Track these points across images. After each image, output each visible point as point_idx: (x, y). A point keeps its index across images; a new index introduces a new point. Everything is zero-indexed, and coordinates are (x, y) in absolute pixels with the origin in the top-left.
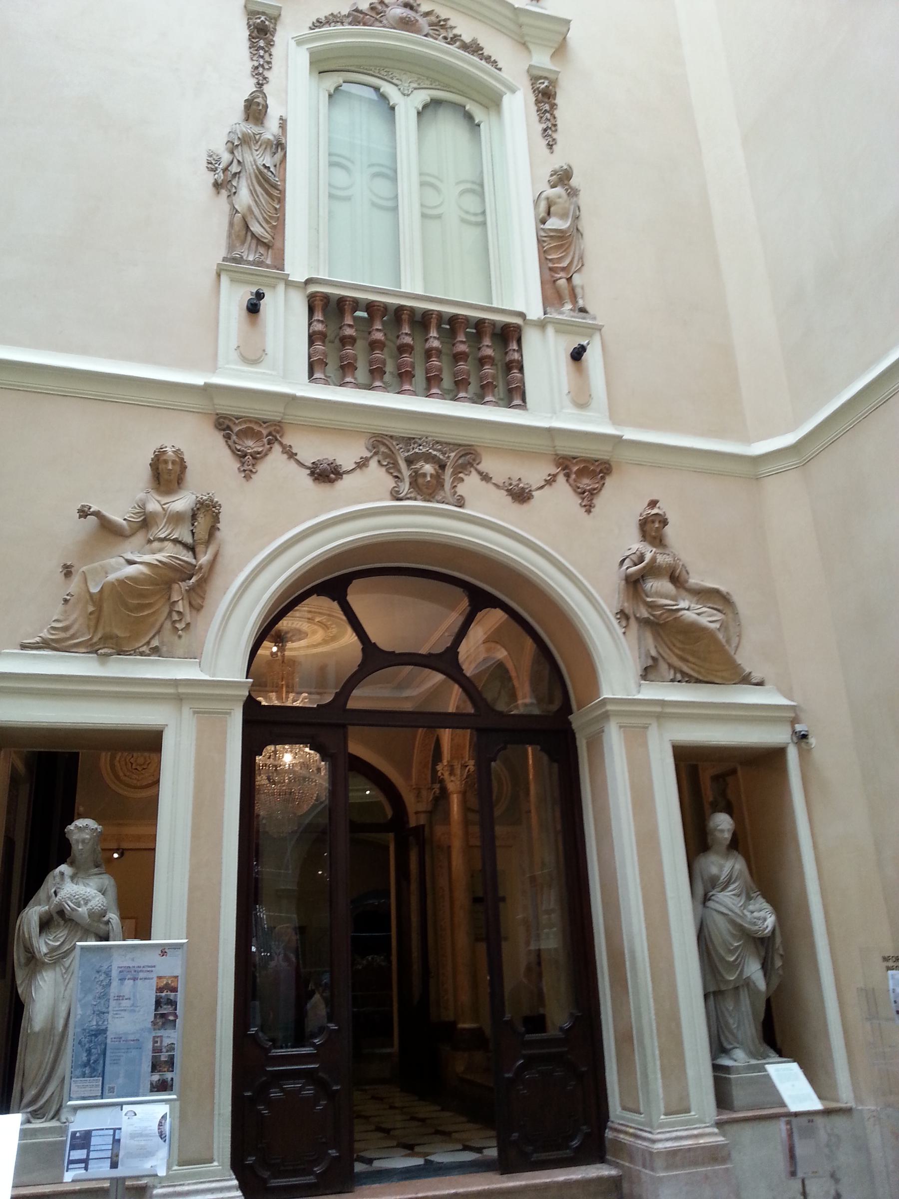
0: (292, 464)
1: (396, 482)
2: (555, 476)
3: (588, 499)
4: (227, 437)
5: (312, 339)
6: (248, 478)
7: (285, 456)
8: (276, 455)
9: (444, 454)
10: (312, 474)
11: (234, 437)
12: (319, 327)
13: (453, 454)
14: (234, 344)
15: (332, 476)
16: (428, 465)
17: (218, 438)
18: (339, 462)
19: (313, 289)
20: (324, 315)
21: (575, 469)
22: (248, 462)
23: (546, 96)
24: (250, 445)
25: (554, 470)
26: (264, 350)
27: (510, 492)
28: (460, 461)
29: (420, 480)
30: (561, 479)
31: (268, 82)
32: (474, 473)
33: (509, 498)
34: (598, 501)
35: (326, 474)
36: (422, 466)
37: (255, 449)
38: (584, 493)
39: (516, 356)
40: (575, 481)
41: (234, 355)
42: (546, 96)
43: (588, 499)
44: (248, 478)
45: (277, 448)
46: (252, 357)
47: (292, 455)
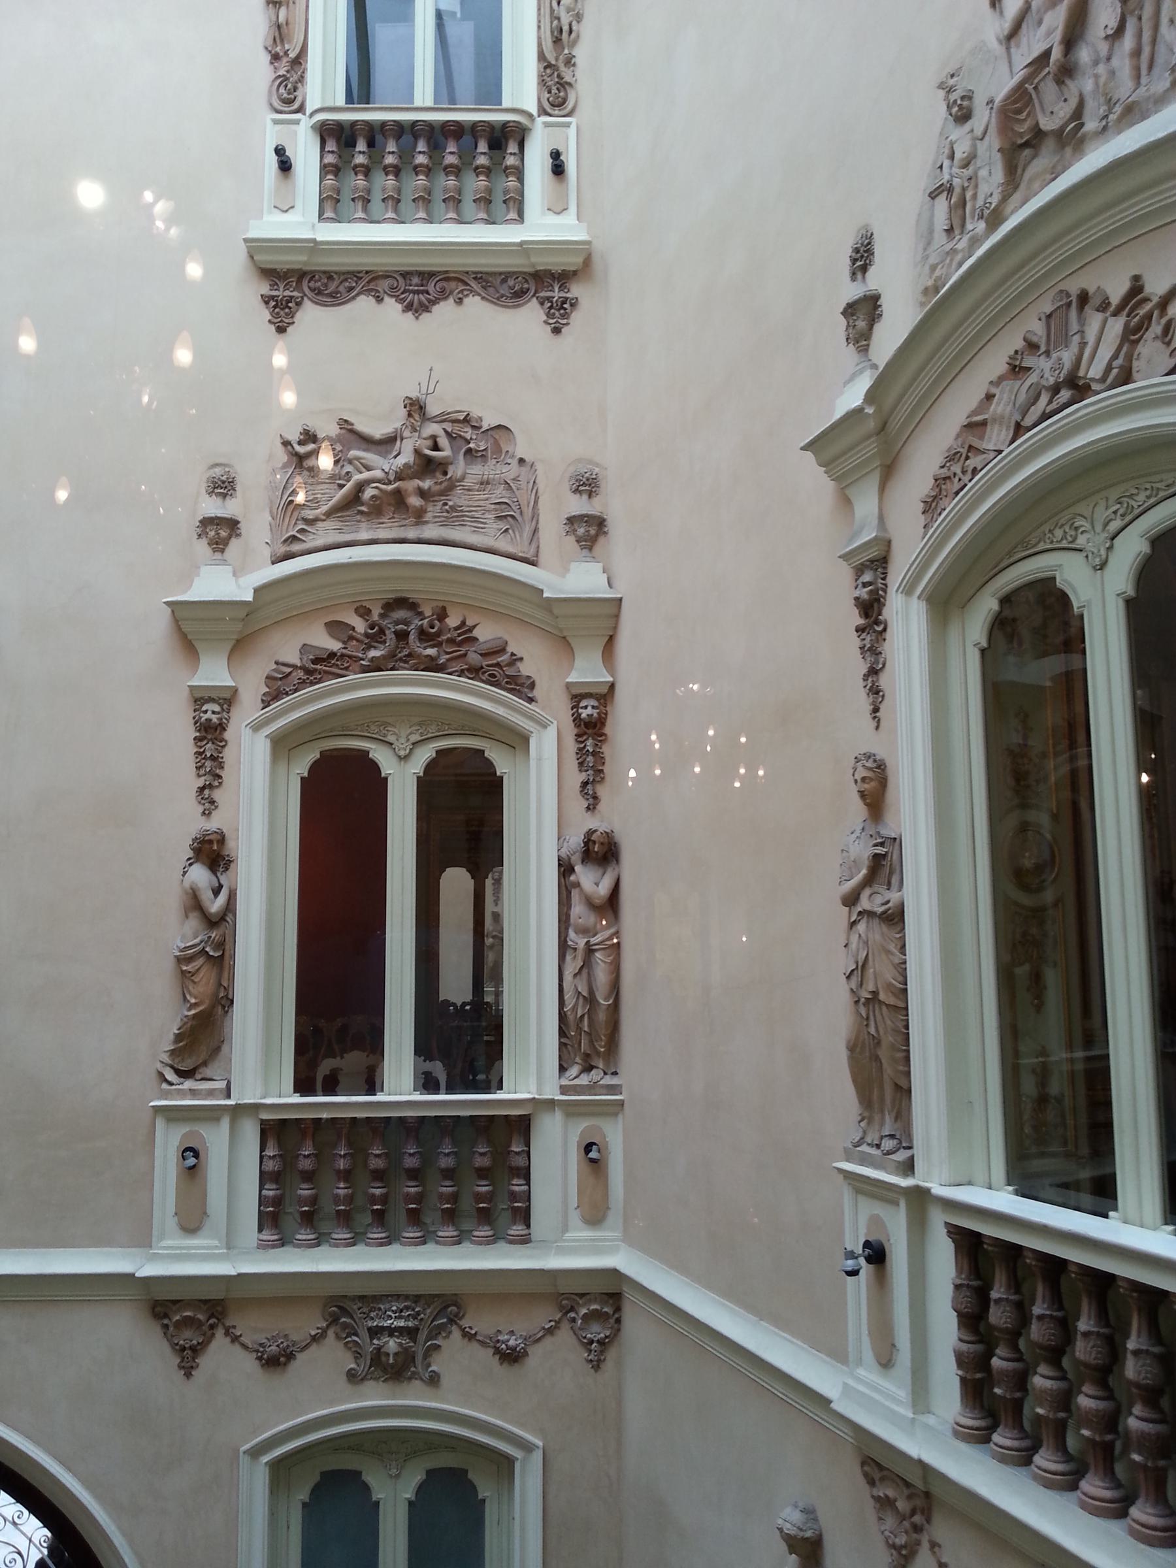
0: (237, 1348)
1: (356, 1358)
2: (558, 1322)
3: (598, 1353)
4: (166, 1327)
5: (264, 1177)
6: (188, 1375)
7: (228, 1339)
8: (220, 1340)
9: (415, 1318)
10: (260, 1359)
11: (171, 1329)
12: (270, 1166)
13: (428, 1311)
14: (171, 1207)
15: (282, 1359)
16: (397, 1331)
17: (155, 1331)
18: (295, 1337)
19: (265, 1116)
20: (280, 1147)
21: (584, 1311)
22: (188, 1358)
23: (591, 729)
24: (189, 1337)
25: (558, 1316)
26: (205, 1213)
27: (497, 1351)
28: (435, 1323)
29: (383, 1359)
30: (565, 1326)
31: (216, 807)
32: (456, 1334)
33: (497, 1357)
34: (611, 1354)
35: (276, 1360)
36: (387, 1342)
37: (195, 1342)
38: (592, 1342)
39: (520, 1162)
40: (580, 1329)
41: (172, 1223)
42: (591, 729)
43: (598, 1353)
44: (188, 1375)
45: (220, 1333)
46: (192, 1220)
47: (235, 1339)
